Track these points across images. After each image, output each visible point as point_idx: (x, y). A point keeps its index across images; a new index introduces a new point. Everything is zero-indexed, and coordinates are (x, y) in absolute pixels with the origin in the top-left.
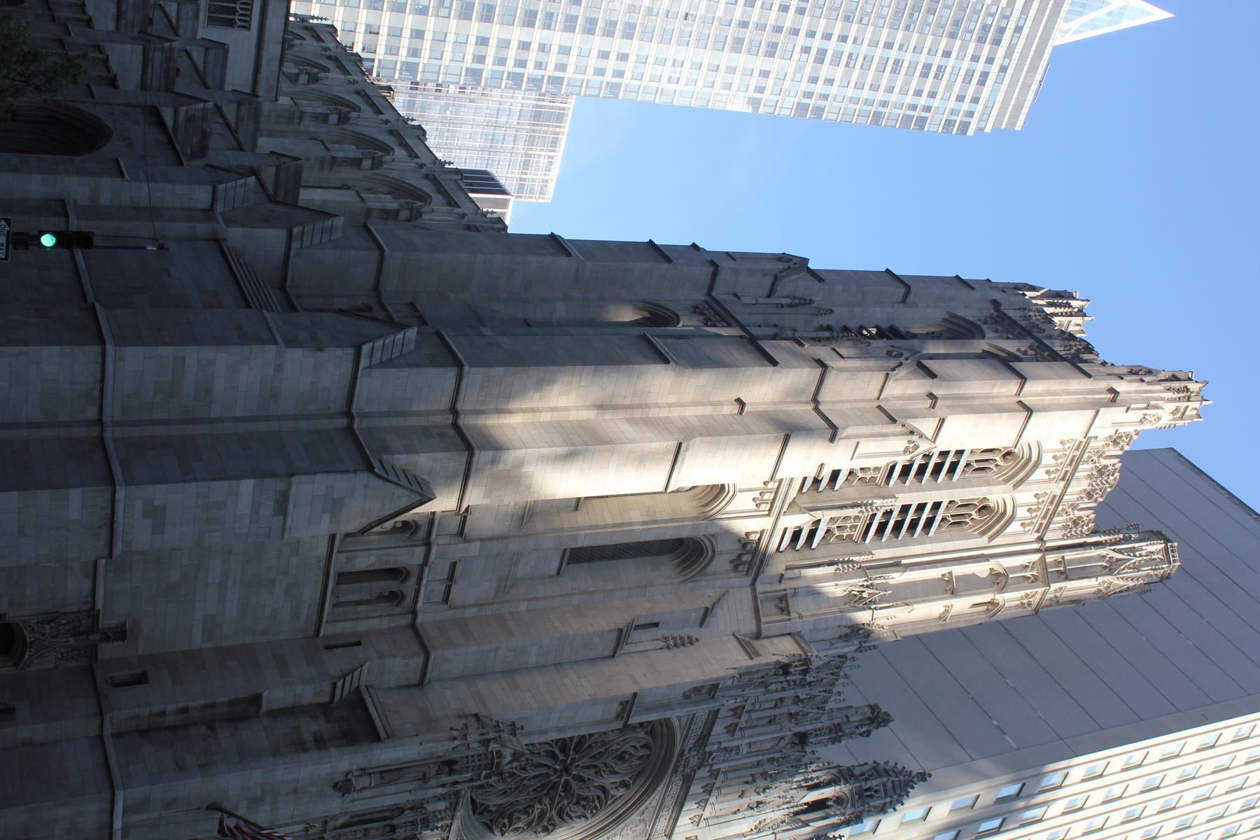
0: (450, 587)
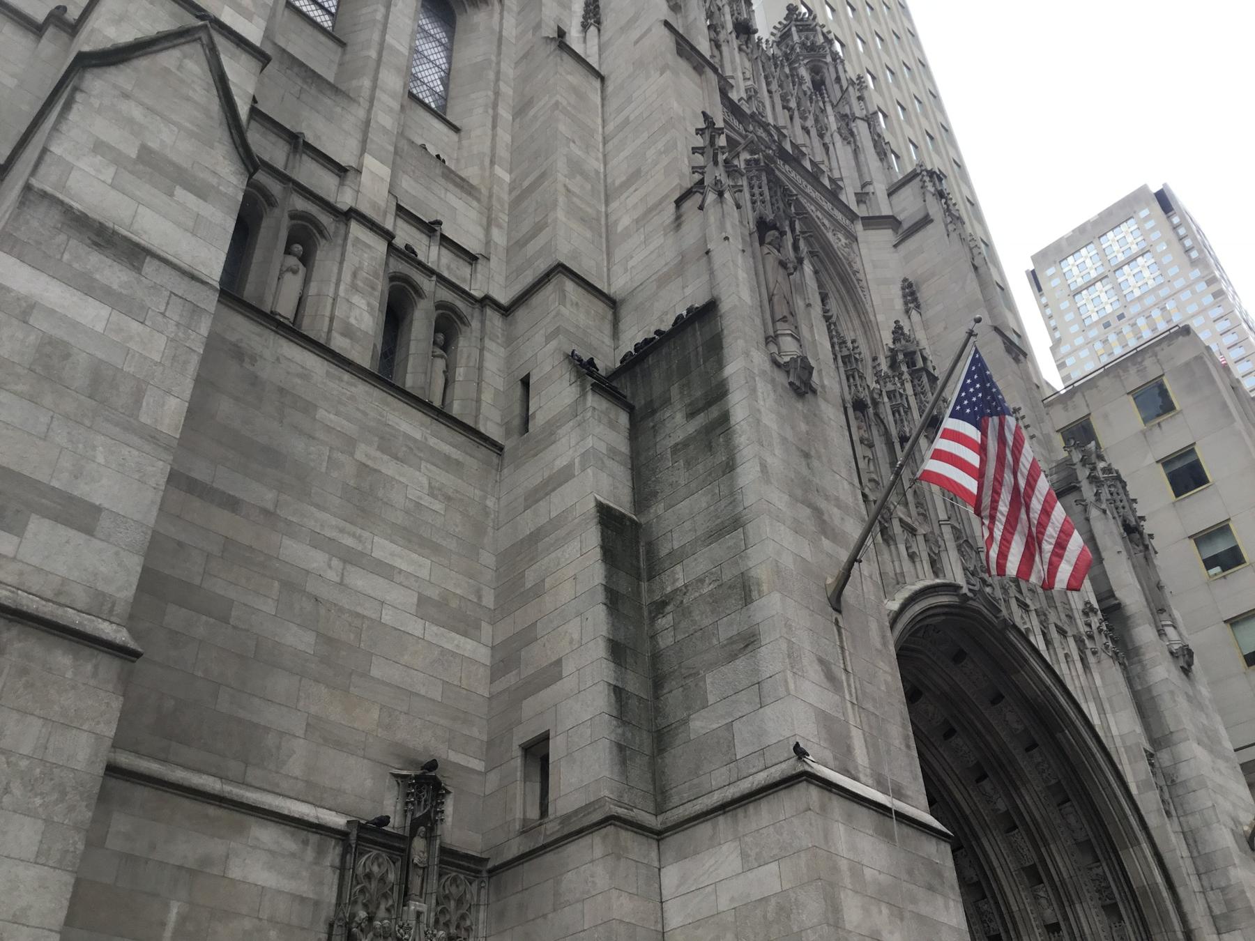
0: (443, 238)
